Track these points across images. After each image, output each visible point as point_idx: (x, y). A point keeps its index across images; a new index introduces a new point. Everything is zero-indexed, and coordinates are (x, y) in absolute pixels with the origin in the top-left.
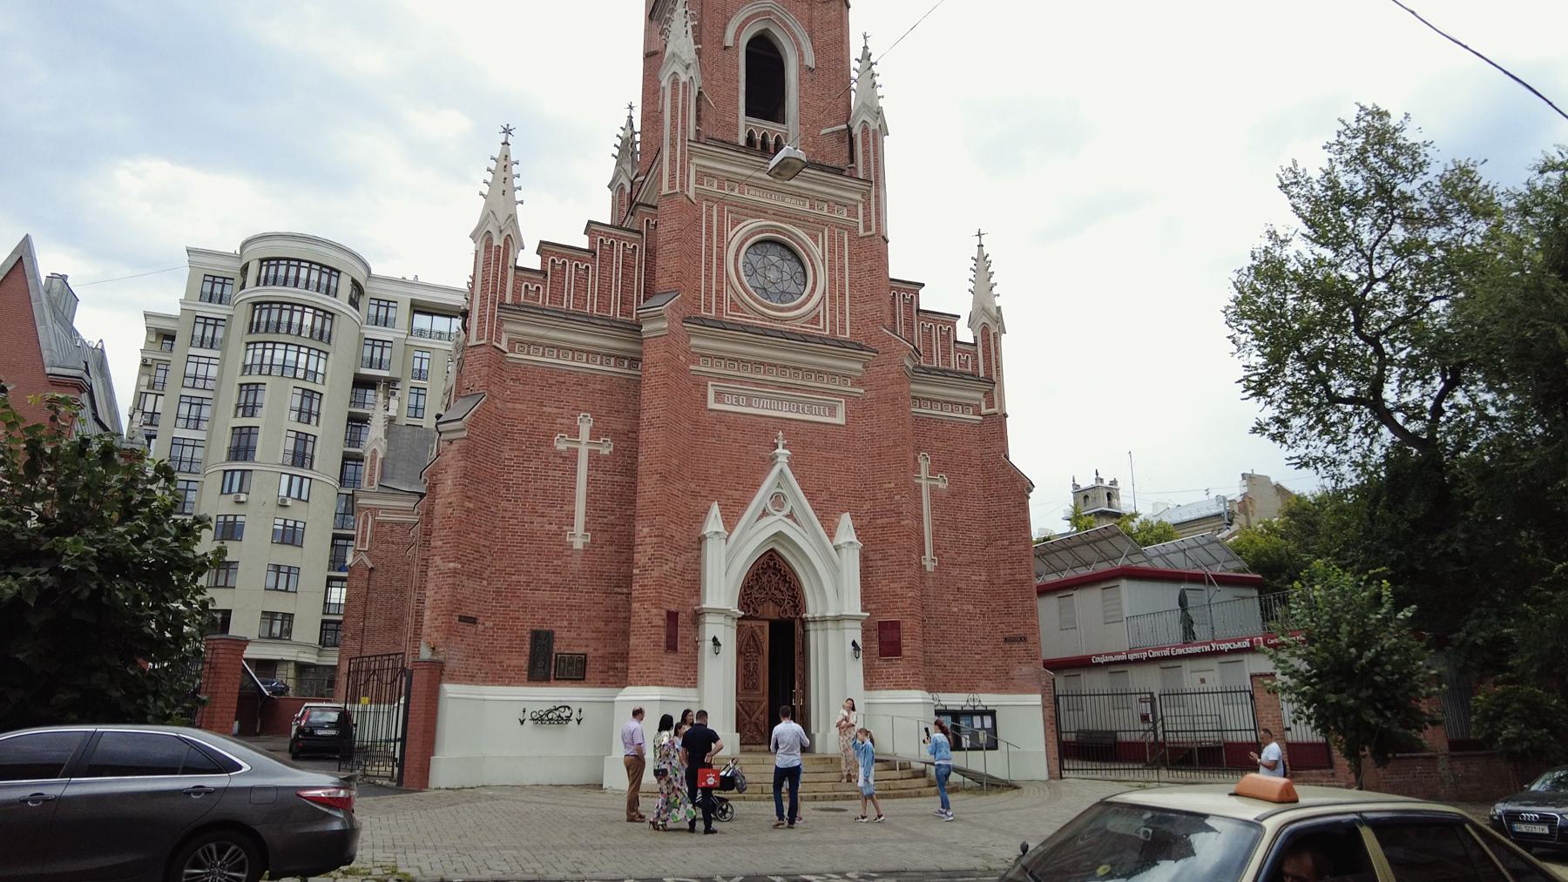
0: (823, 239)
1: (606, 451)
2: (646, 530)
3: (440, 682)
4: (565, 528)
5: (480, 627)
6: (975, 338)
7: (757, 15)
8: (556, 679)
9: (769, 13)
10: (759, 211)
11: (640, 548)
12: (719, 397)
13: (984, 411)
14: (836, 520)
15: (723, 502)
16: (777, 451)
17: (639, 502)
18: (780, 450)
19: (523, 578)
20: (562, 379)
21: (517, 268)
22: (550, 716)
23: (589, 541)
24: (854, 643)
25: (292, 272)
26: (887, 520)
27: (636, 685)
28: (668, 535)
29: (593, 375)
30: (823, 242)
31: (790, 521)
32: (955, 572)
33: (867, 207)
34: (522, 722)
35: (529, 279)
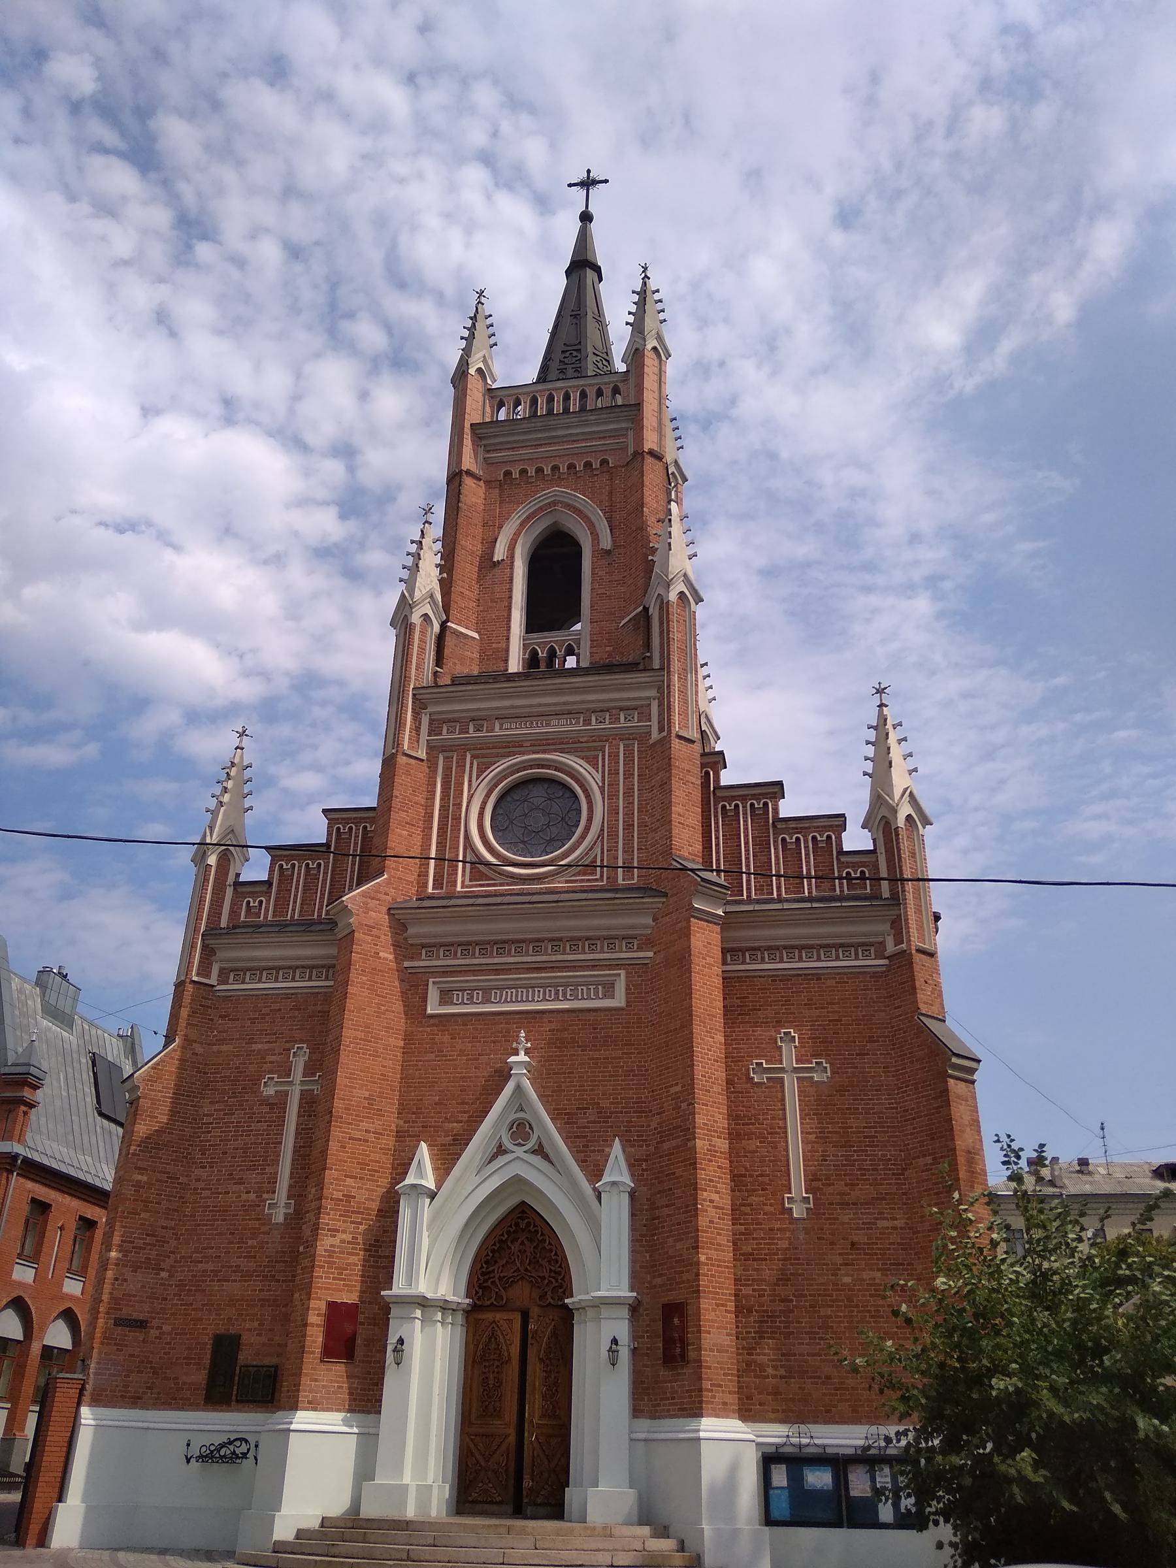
0: (603, 759)
3: (79, 1404)
4: (265, 1196)
5: (153, 1333)
6: (874, 840)
7: (541, 508)
8: (237, 1401)
9: (554, 503)
10: (512, 746)
12: (446, 997)
13: (891, 948)
14: (607, 1150)
15: (440, 1140)
16: (513, 1059)
18: (522, 1057)
19: (210, 1266)
20: (277, 1006)
21: (237, 884)
22: (222, 1453)
23: (291, 1211)
24: (615, 1341)
26: (674, 1143)
28: (339, 1195)
29: (314, 995)
30: (604, 762)
31: (536, 1160)
32: (846, 1217)
33: (660, 705)
34: (188, 1461)
35: (253, 894)
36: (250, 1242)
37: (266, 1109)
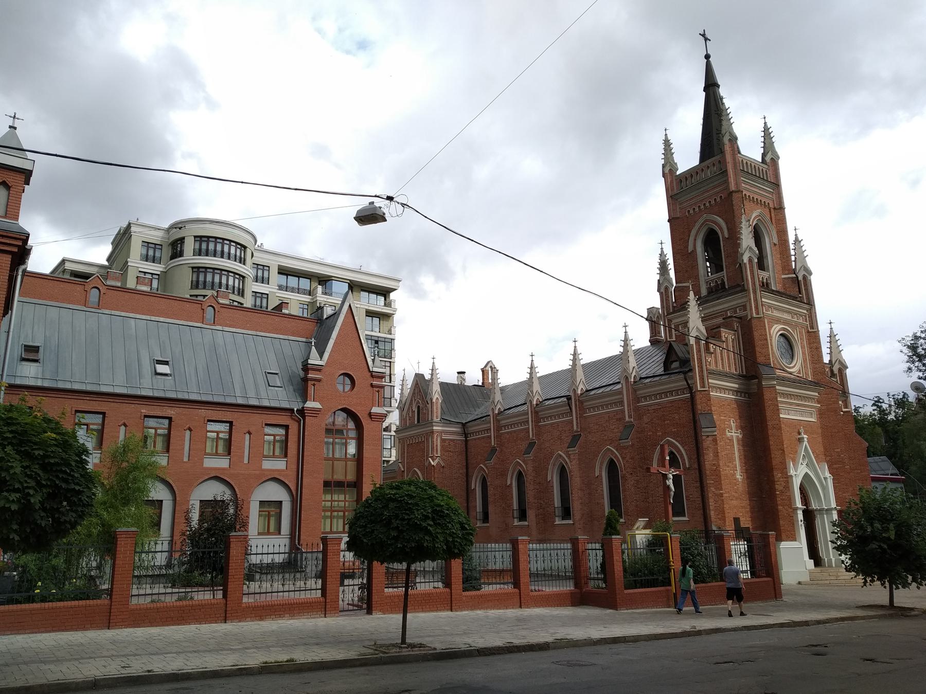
1: (740, 436)
2: (780, 475)
10: (778, 321)
11: (779, 483)
17: (774, 463)
19: (727, 495)
25: (219, 247)
26: (837, 466)
27: (786, 541)
36: (735, 487)
37: (728, 441)
